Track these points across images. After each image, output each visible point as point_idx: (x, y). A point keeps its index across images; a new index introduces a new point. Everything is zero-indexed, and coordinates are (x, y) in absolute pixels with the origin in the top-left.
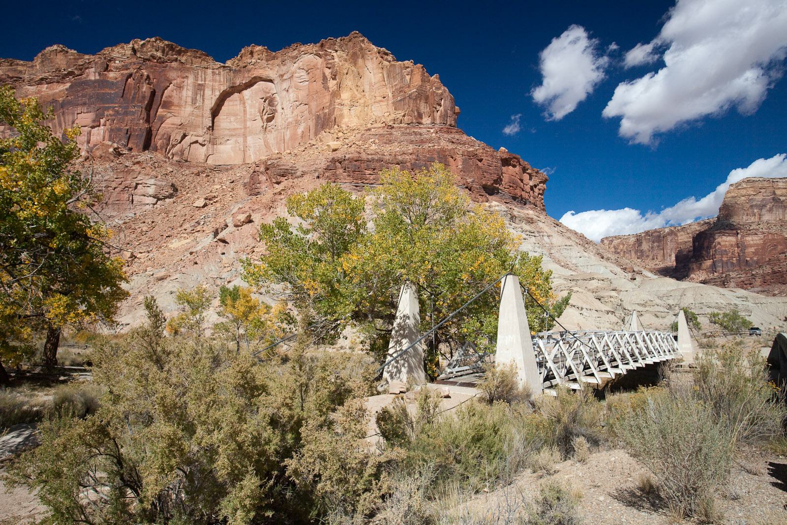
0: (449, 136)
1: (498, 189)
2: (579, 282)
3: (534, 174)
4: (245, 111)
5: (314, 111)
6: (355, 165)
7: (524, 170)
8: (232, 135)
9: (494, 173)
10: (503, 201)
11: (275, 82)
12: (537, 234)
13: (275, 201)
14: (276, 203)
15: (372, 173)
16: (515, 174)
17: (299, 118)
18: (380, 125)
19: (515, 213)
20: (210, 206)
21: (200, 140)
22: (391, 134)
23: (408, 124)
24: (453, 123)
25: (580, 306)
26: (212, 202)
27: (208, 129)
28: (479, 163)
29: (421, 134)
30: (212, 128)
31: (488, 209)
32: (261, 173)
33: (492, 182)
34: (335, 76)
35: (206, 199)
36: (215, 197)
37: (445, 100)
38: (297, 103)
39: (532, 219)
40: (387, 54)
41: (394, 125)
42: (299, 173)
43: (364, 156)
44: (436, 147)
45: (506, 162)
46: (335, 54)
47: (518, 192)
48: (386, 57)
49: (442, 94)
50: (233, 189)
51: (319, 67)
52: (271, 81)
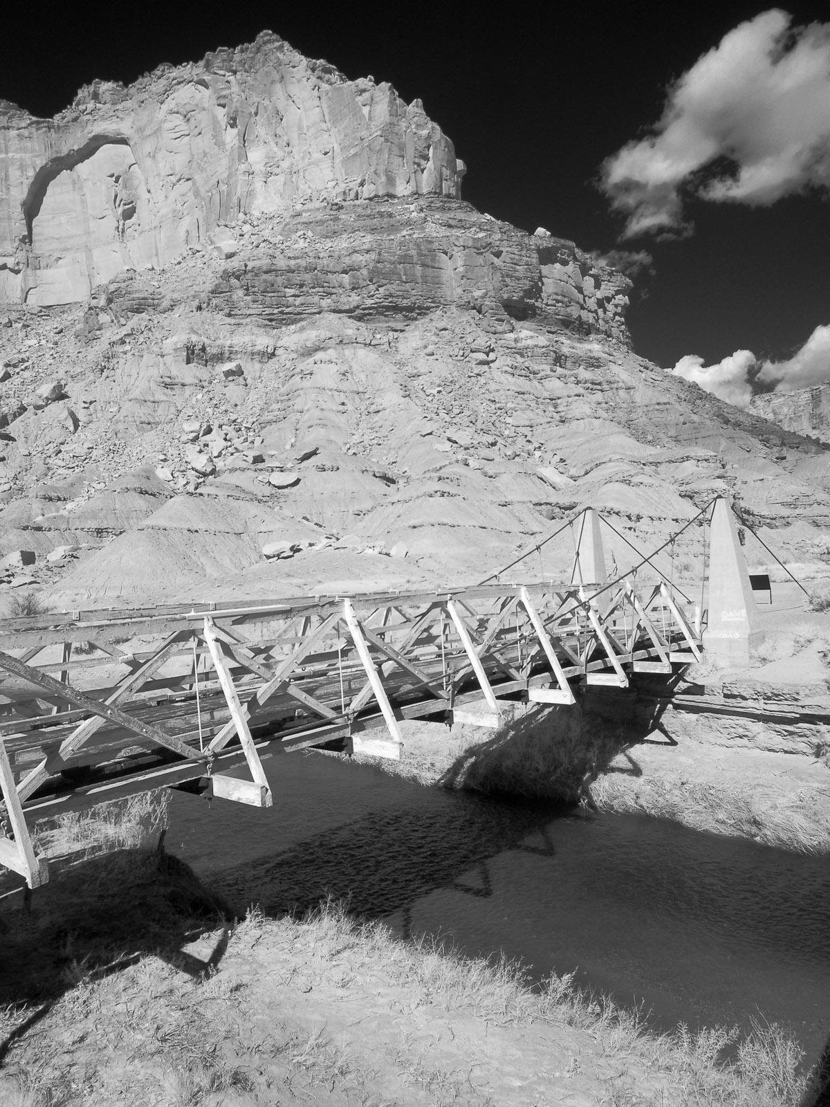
0: (446, 216)
1: (533, 308)
2: (662, 468)
3: (607, 278)
4: (83, 202)
5: (202, 191)
6: (265, 281)
7: (585, 270)
8: (66, 250)
9: (526, 278)
10: (545, 330)
11: (132, 143)
12: (605, 387)
13: (113, 356)
14: (115, 360)
15: (297, 292)
16: (565, 278)
17: (179, 207)
18: (317, 204)
19: (565, 350)
20: (16, 376)
21: (10, 262)
22: (336, 219)
23: (371, 199)
24: (453, 191)
25: (634, 512)
26: (17, 370)
27: (23, 240)
28: (495, 260)
29: (390, 215)
30: (28, 239)
31: (513, 345)
32: (102, 310)
33: (521, 294)
34: (234, 119)
35: (7, 365)
36: (23, 361)
37: (435, 149)
38: (174, 179)
39: (597, 359)
40: (329, 71)
41: (344, 204)
42: (166, 304)
43: (281, 263)
44: (415, 236)
45: (547, 256)
46: (232, 78)
47: (574, 311)
48: (327, 76)
49: (429, 137)
50: (56, 343)
51: (206, 105)
52: (124, 141)
